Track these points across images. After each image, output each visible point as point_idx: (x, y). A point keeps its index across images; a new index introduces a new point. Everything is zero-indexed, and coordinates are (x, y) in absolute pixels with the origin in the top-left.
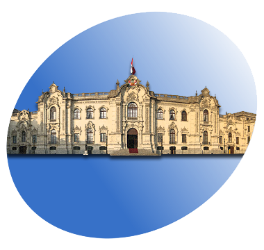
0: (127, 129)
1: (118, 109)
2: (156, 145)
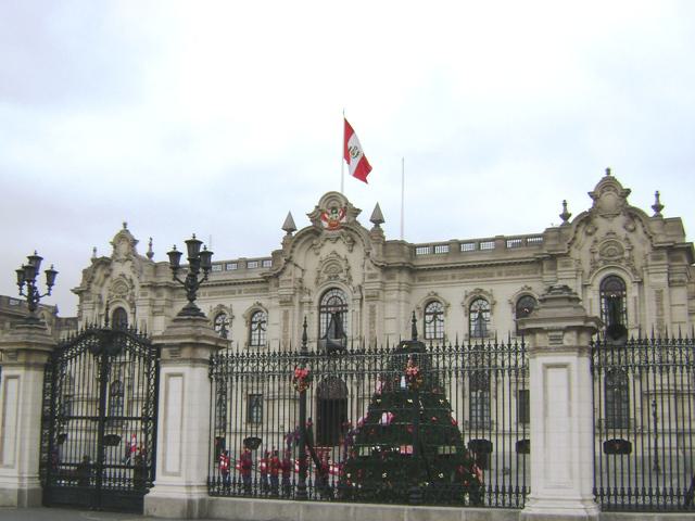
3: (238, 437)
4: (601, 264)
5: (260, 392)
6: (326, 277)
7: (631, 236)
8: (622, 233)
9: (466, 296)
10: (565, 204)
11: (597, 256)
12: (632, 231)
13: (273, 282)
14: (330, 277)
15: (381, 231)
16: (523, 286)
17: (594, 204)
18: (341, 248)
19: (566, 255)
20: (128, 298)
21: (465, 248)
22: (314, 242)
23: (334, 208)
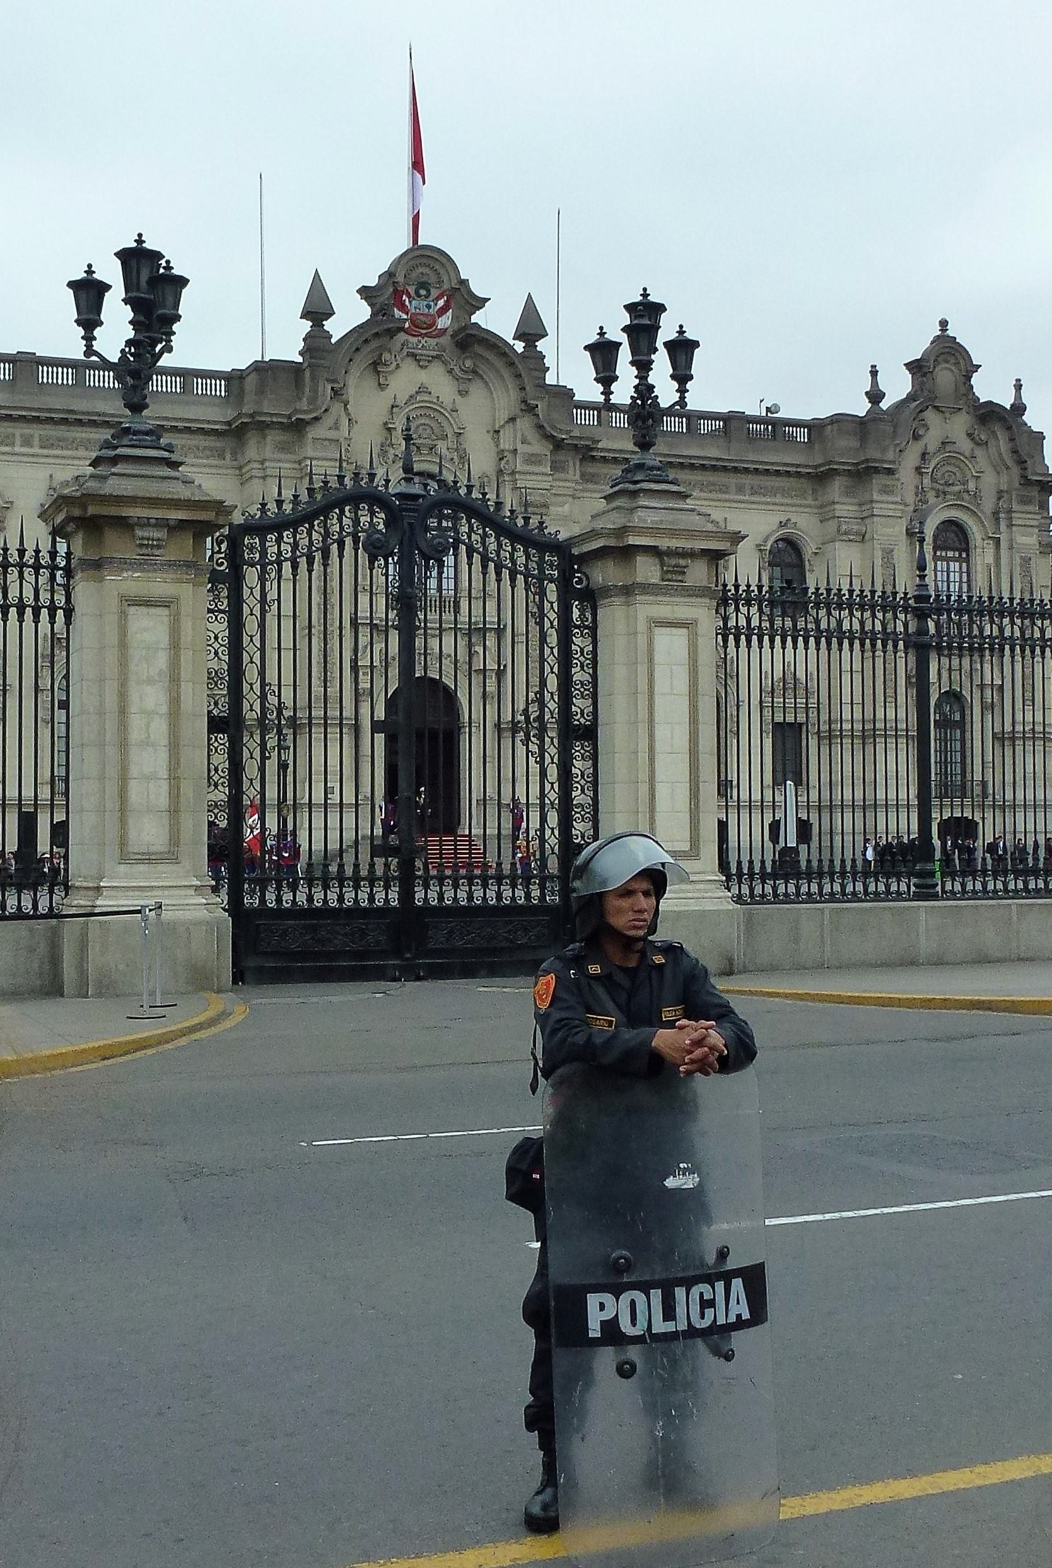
3: (757, 816)
4: (932, 500)
5: (801, 718)
7: (979, 453)
8: (965, 445)
11: (927, 481)
12: (979, 444)
13: (274, 437)
16: (784, 520)
18: (439, 383)
19: (890, 472)
21: (705, 426)
23: (423, 285)
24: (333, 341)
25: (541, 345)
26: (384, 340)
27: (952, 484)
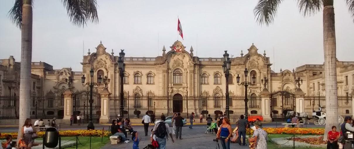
0: (173, 94)
1: (164, 76)
2: (200, 109)
4: (251, 68)
6: (176, 65)
7: (258, 61)
8: (256, 60)
9: (214, 73)
10: (242, 51)
11: (250, 65)
14: (177, 66)
15: (193, 54)
17: (249, 52)
20: (104, 67)
22: (173, 55)
23: (178, 46)
24: (166, 54)
25: (193, 52)
26: (172, 53)
27: (254, 65)
